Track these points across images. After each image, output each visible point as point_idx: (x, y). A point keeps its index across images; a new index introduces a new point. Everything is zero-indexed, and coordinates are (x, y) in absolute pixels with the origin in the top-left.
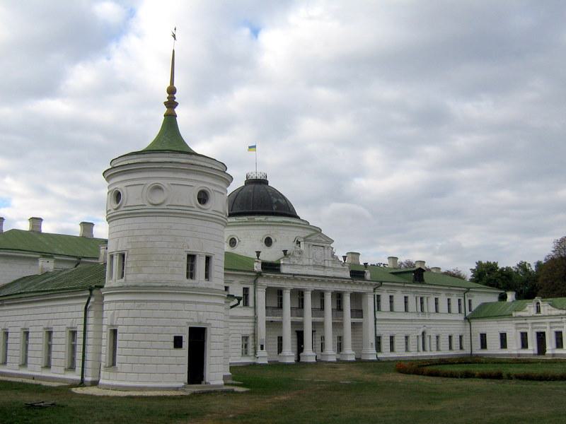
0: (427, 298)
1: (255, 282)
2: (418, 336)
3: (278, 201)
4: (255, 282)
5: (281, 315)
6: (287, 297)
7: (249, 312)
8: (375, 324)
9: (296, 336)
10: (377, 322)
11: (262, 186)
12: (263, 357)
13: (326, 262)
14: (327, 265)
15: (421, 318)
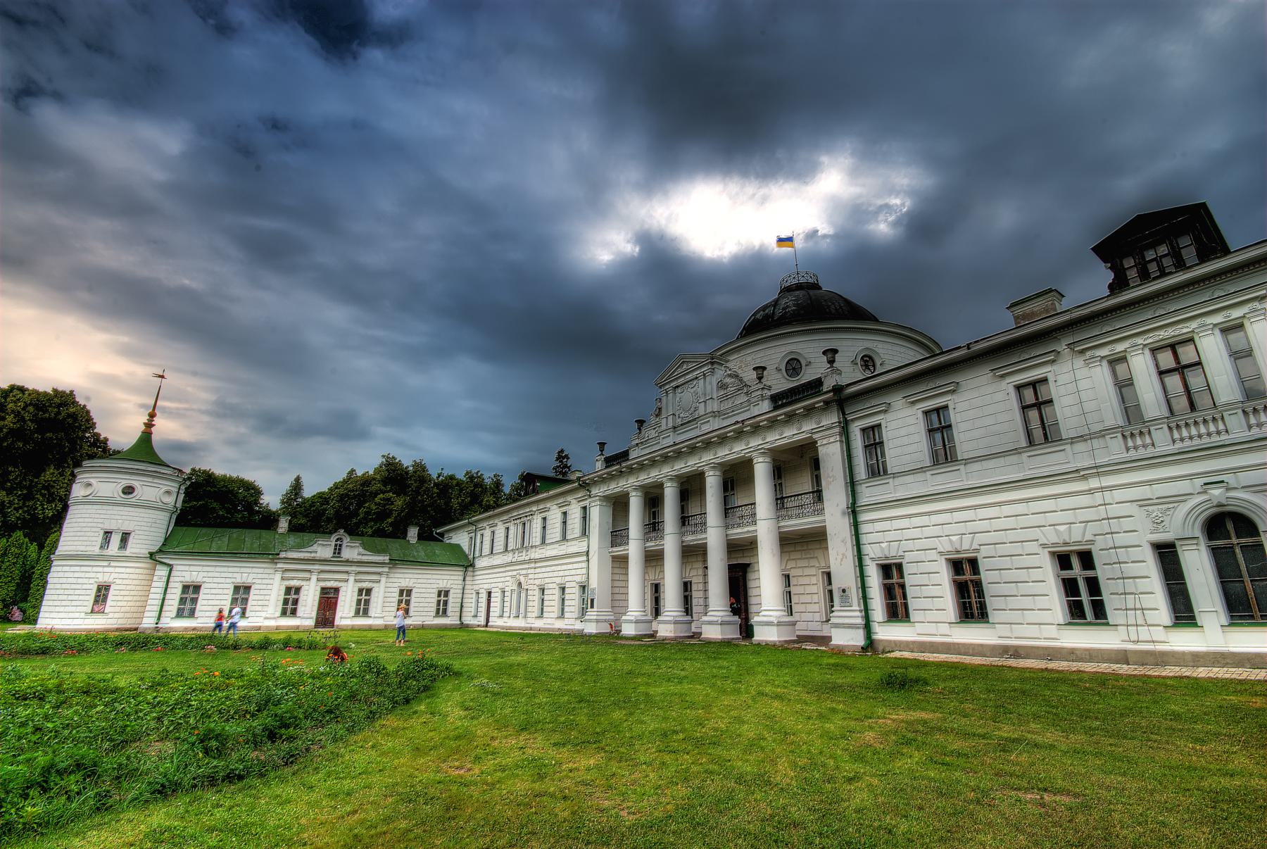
6: (635, 504)
8: (856, 525)
10: (863, 517)
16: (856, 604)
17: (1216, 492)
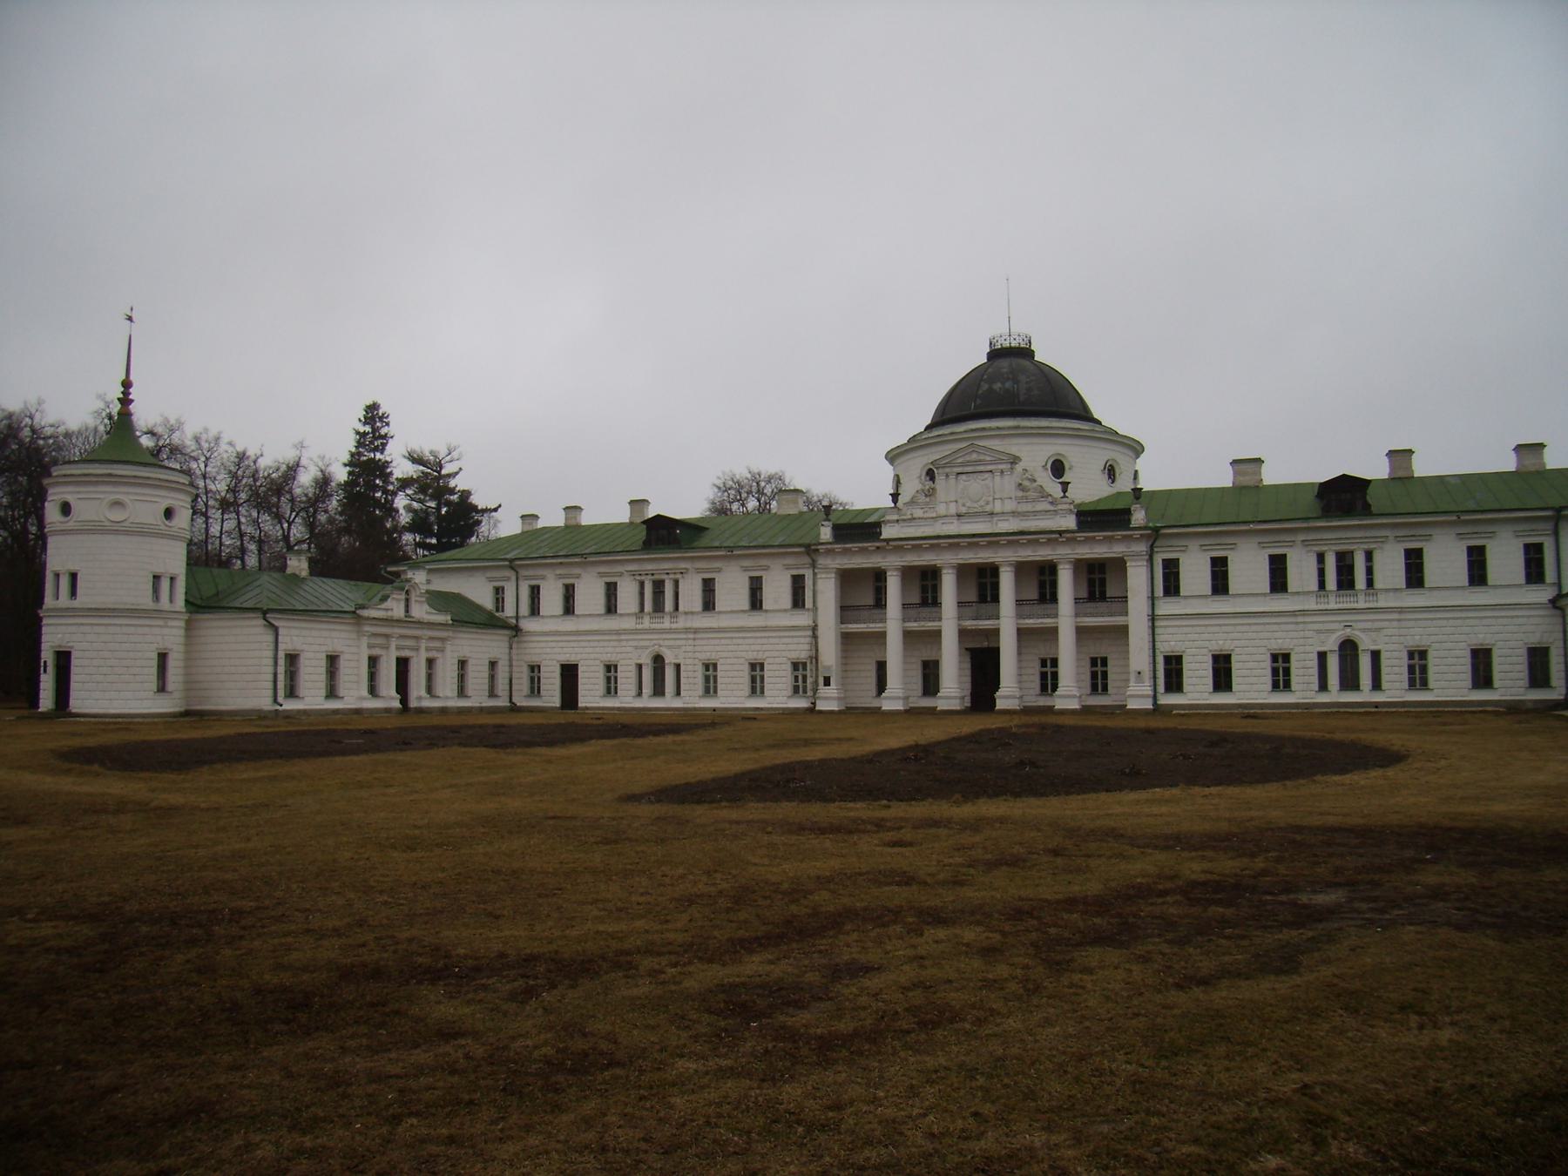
0: (1369, 556)
1: (814, 565)
2: (1322, 656)
3: (991, 390)
4: (814, 565)
5: (884, 620)
7: (802, 619)
8: (1153, 628)
9: (968, 659)
10: (1157, 623)
11: (1025, 363)
12: (829, 700)
13: (998, 503)
14: (998, 507)
15: (1332, 606)
16: (1148, 682)
17: (1348, 630)
